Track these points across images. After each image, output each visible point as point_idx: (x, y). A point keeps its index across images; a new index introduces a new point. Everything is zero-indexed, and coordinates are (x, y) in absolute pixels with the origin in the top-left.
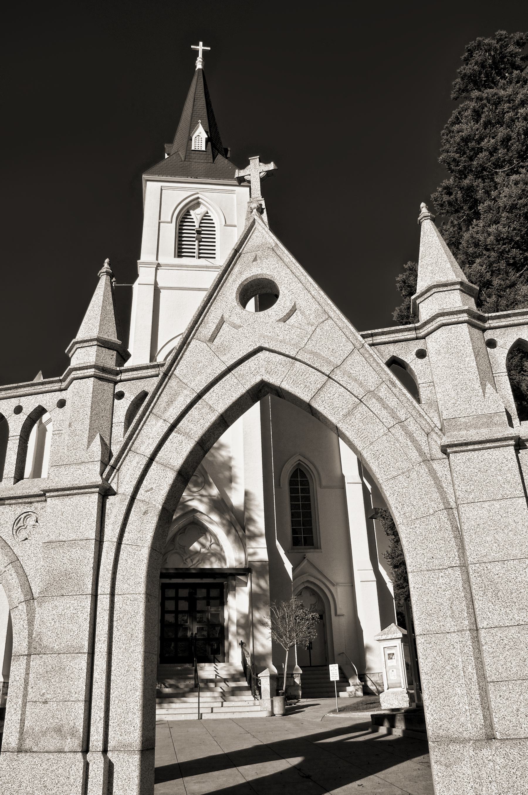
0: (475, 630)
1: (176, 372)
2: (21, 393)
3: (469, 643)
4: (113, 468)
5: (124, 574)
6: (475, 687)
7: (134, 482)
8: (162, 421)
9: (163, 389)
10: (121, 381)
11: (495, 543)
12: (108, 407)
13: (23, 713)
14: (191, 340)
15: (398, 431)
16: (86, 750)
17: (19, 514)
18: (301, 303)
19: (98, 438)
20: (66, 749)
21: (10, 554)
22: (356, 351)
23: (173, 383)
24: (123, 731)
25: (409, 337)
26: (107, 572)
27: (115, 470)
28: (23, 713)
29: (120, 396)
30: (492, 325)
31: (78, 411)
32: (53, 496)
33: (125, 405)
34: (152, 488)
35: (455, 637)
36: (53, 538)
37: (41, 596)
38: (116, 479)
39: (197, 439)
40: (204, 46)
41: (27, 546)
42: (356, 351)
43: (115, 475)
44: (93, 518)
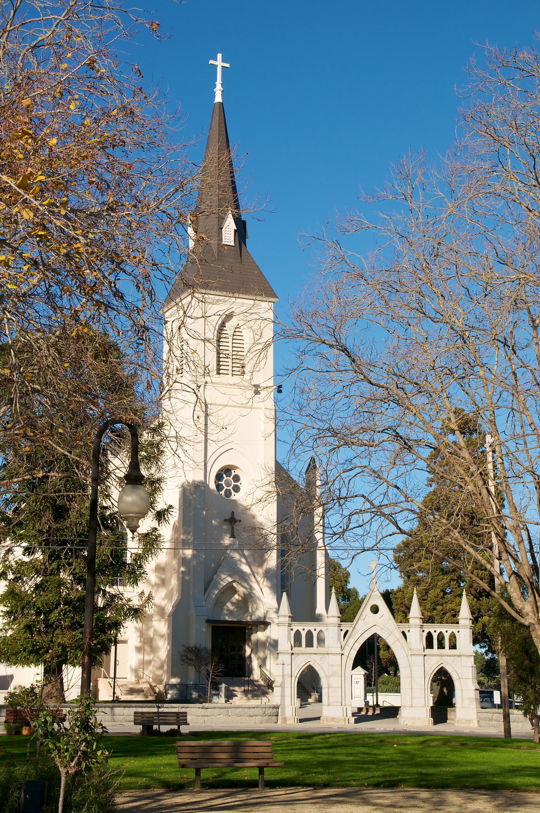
15: (402, 649)
23: (355, 630)
29: (341, 630)
40: (223, 61)
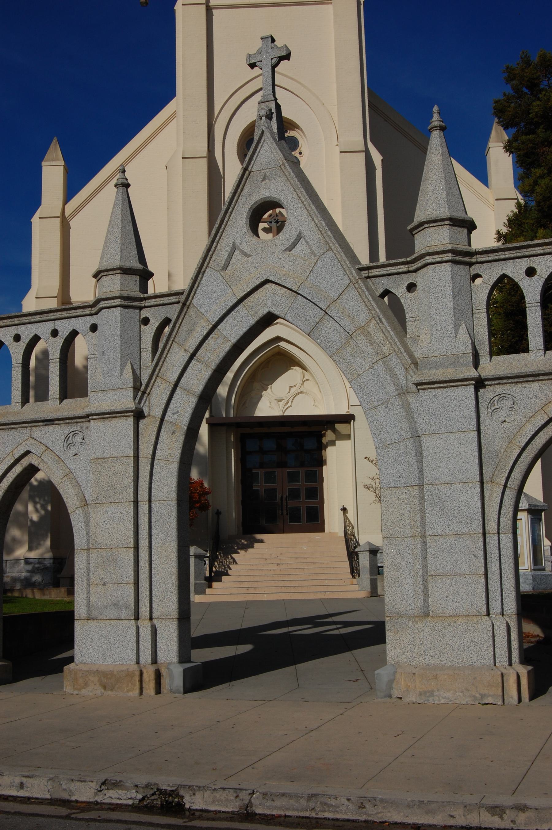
0: (423, 536)
1: (194, 301)
2: (55, 317)
3: (419, 546)
4: (144, 393)
5: (159, 484)
6: (420, 579)
7: (163, 407)
8: (183, 350)
9: (183, 318)
10: (145, 307)
11: (447, 468)
12: (136, 334)
13: (88, 593)
14: (206, 268)
15: (380, 368)
16: (137, 618)
17: (67, 433)
18: (306, 233)
19: (129, 364)
20: (122, 618)
21: (64, 467)
22: (351, 285)
23: (191, 312)
24: (164, 605)
25: (401, 270)
26: (144, 483)
27: (146, 395)
28: (88, 593)
29: (146, 321)
30: (479, 260)
31: (109, 340)
32: (95, 419)
33: (151, 331)
34: (178, 412)
35: (409, 541)
36: (98, 455)
37: (93, 503)
38: (147, 403)
39: (214, 367)
41: (78, 461)
42: (351, 285)
43: (146, 399)
44: (130, 438)
